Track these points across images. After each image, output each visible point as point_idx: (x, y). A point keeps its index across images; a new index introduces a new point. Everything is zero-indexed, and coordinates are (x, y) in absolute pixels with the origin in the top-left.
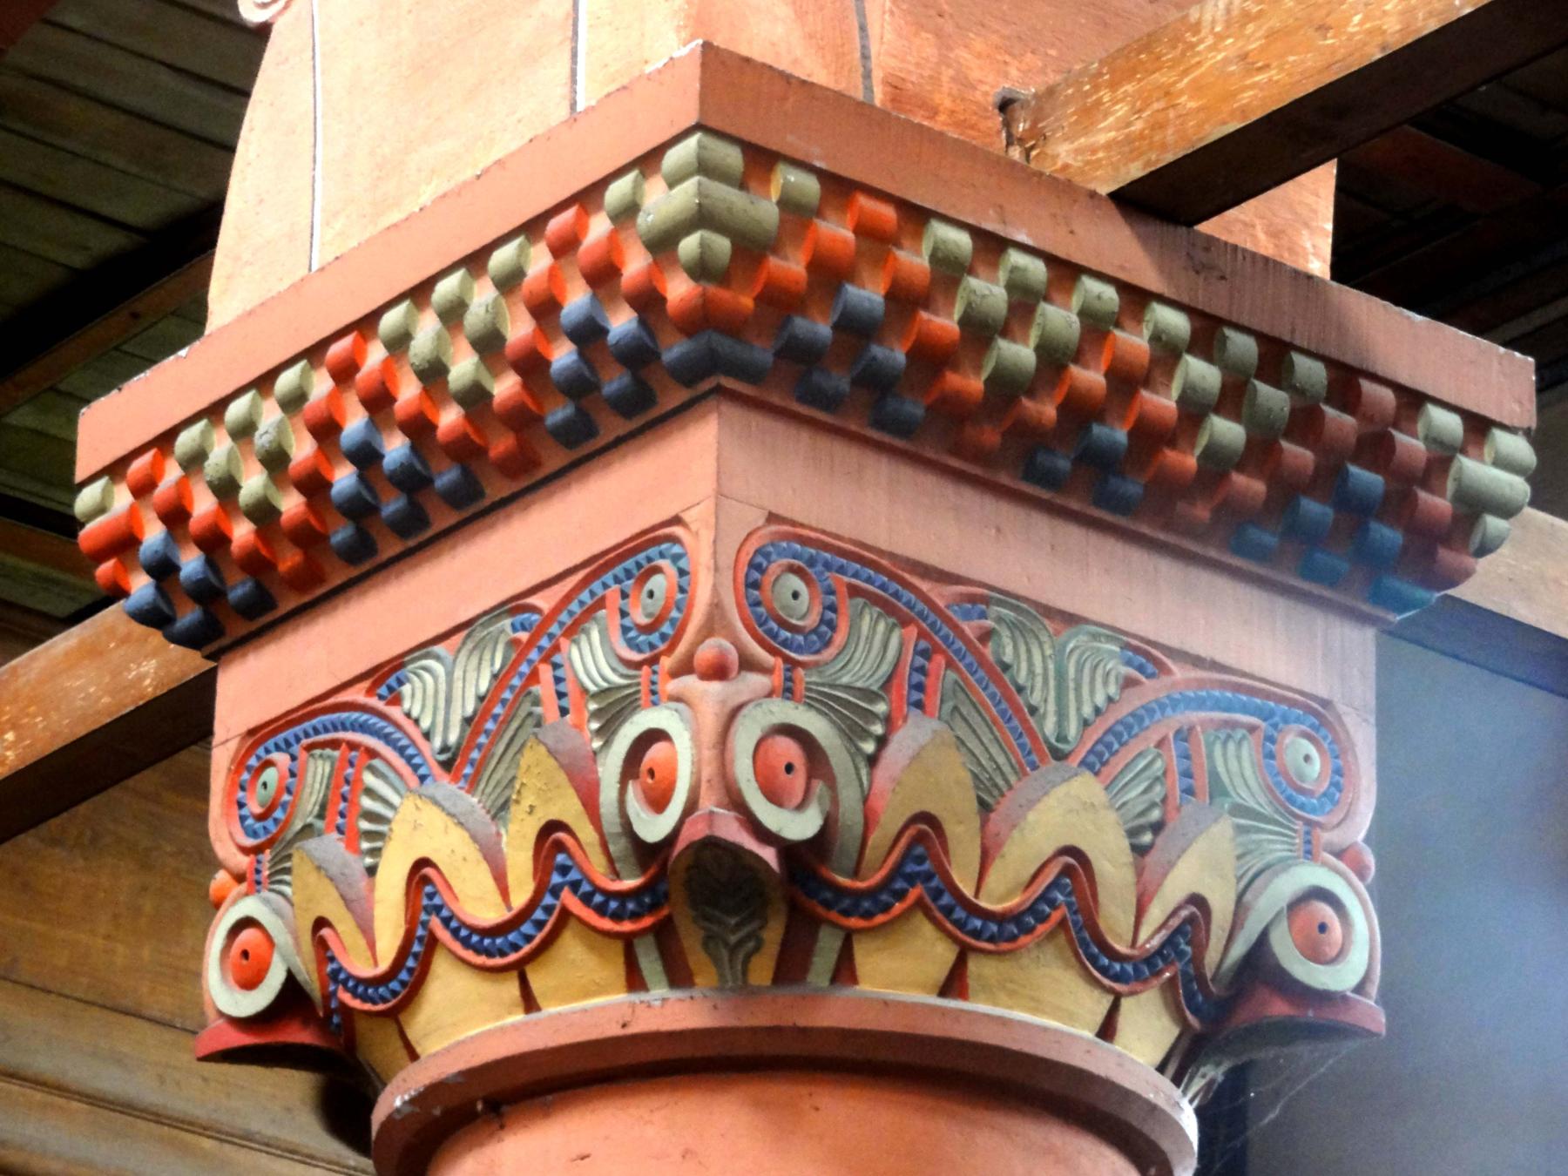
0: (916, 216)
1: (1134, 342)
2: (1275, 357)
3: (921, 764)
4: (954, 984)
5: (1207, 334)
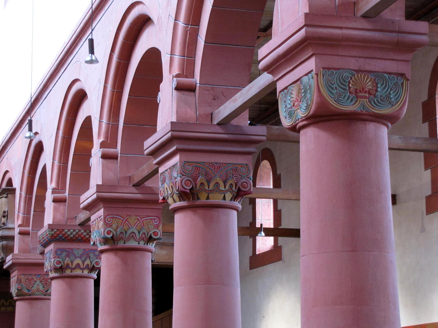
0: (63, 230)
1: (80, 233)
3: (67, 261)
4: (71, 272)
5: (85, 231)
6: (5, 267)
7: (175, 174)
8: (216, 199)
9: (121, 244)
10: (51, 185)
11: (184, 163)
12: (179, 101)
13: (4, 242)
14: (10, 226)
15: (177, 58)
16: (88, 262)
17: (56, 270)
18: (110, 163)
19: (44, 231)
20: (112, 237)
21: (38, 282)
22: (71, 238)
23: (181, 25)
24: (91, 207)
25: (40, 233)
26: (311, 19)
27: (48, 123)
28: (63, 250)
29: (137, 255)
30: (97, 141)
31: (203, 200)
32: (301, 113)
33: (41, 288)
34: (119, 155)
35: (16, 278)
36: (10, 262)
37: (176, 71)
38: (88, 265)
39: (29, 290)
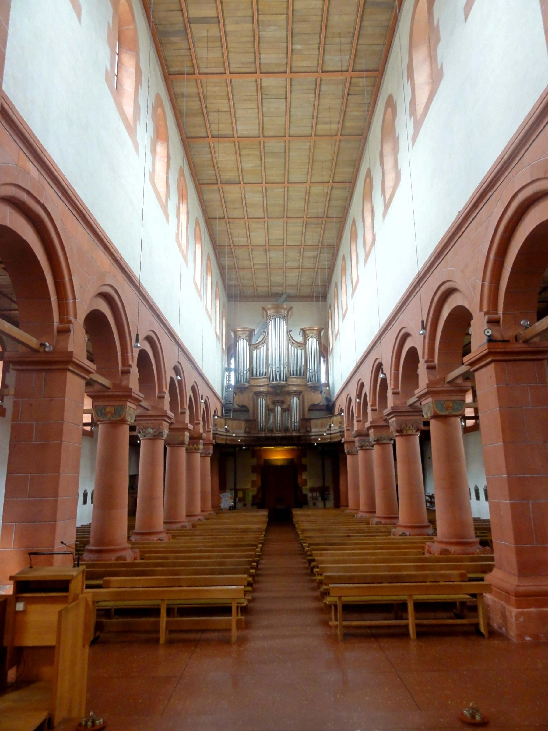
7: (394, 424)
8: (410, 432)
9: (380, 442)
10: (355, 415)
11: (397, 420)
12: (394, 398)
13: (341, 433)
15: (392, 382)
17: (360, 447)
18: (375, 412)
19: (354, 432)
23: (393, 371)
24: (369, 428)
26: (428, 386)
27: (353, 390)
29: (387, 445)
30: (369, 404)
31: (405, 433)
32: (429, 415)
37: (392, 387)
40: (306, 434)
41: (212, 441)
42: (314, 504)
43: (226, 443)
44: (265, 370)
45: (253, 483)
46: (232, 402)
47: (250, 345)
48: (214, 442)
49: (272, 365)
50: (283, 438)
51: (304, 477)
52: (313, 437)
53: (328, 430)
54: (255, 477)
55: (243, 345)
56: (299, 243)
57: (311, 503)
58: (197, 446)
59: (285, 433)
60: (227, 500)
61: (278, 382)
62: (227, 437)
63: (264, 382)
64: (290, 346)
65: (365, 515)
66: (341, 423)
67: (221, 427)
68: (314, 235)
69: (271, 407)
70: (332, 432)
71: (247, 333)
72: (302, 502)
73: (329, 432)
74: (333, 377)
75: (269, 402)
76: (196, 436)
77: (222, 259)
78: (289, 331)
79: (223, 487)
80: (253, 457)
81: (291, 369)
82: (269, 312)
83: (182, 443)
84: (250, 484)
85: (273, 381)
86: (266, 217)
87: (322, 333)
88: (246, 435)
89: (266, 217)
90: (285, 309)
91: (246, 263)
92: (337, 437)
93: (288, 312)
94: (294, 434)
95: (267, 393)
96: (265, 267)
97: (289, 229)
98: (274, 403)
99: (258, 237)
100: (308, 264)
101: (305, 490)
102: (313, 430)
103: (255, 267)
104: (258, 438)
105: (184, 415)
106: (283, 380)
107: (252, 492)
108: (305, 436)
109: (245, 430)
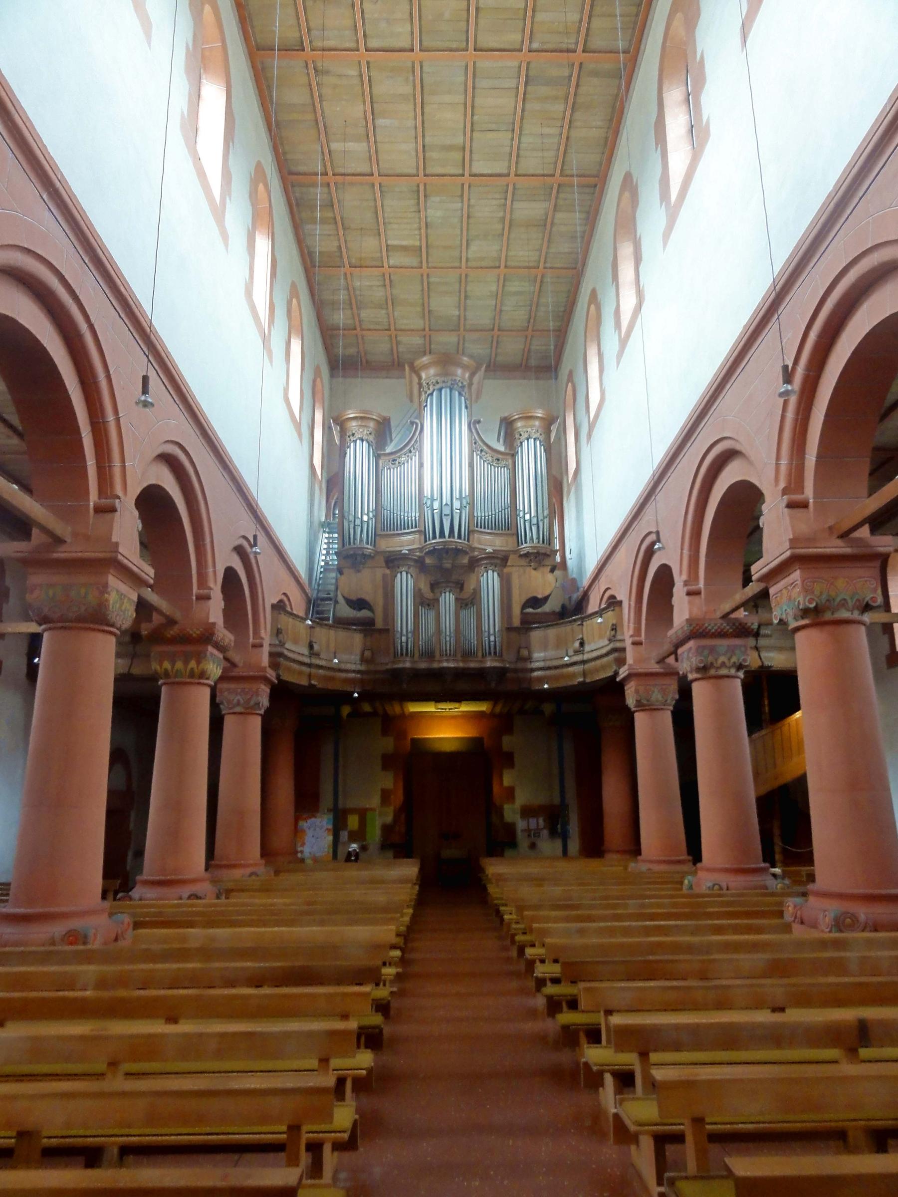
2: (734, 624)
3: (710, 659)
6: (618, 680)
9: (828, 616)
10: (679, 579)
13: (616, 655)
14: (619, 637)
16: (734, 659)
20: (816, 607)
21: (656, 692)
22: (713, 634)
25: (671, 633)
28: (704, 647)
29: (852, 628)
33: (660, 697)
34: (811, 501)
35: (633, 689)
36: (625, 674)
38: (734, 663)
39: (648, 701)
40: (520, 665)
41: (264, 669)
42: (533, 846)
43: (312, 686)
44: (415, 514)
45: (386, 796)
46: (332, 595)
47: (378, 457)
48: (271, 674)
49: (433, 500)
50: (460, 674)
51: (508, 779)
52: (536, 674)
53: (576, 652)
54: (388, 781)
55: (359, 458)
56: (500, 167)
57: (523, 842)
58: (198, 663)
59: (463, 661)
60: (317, 836)
61: (447, 539)
62: (313, 671)
63: (413, 542)
64: (477, 459)
65: (724, 880)
66: (614, 628)
67: (296, 642)
68: (546, 130)
69: (428, 594)
70: (586, 657)
71: (372, 424)
72: (502, 842)
73: (578, 658)
74: (580, 537)
75: (424, 587)
76: (195, 632)
77: (309, 227)
78: (473, 424)
79: (306, 801)
80: (385, 732)
81: (478, 513)
82: (423, 375)
83: (96, 619)
84: (374, 795)
85: (434, 537)
86: (417, 48)
87: (554, 428)
88: (362, 668)
89: (417, 48)
90: (465, 367)
91: (369, 245)
92: (603, 668)
93: (472, 375)
94: (489, 663)
95: (420, 564)
96: (414, 262)
97: (478, 101)
98: (433, 586)
99: (400, 153)
100: (523, 251)
101: (511, 813)
102: (538, 655)
103: (392, 262)
104: (396, 675)
105: (108, 516)
106: (459, 537)
107: (381, 818)
108: (516, 671)
109: (363, 654)
